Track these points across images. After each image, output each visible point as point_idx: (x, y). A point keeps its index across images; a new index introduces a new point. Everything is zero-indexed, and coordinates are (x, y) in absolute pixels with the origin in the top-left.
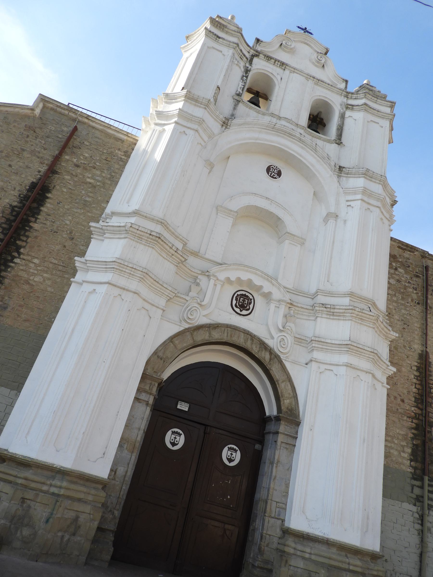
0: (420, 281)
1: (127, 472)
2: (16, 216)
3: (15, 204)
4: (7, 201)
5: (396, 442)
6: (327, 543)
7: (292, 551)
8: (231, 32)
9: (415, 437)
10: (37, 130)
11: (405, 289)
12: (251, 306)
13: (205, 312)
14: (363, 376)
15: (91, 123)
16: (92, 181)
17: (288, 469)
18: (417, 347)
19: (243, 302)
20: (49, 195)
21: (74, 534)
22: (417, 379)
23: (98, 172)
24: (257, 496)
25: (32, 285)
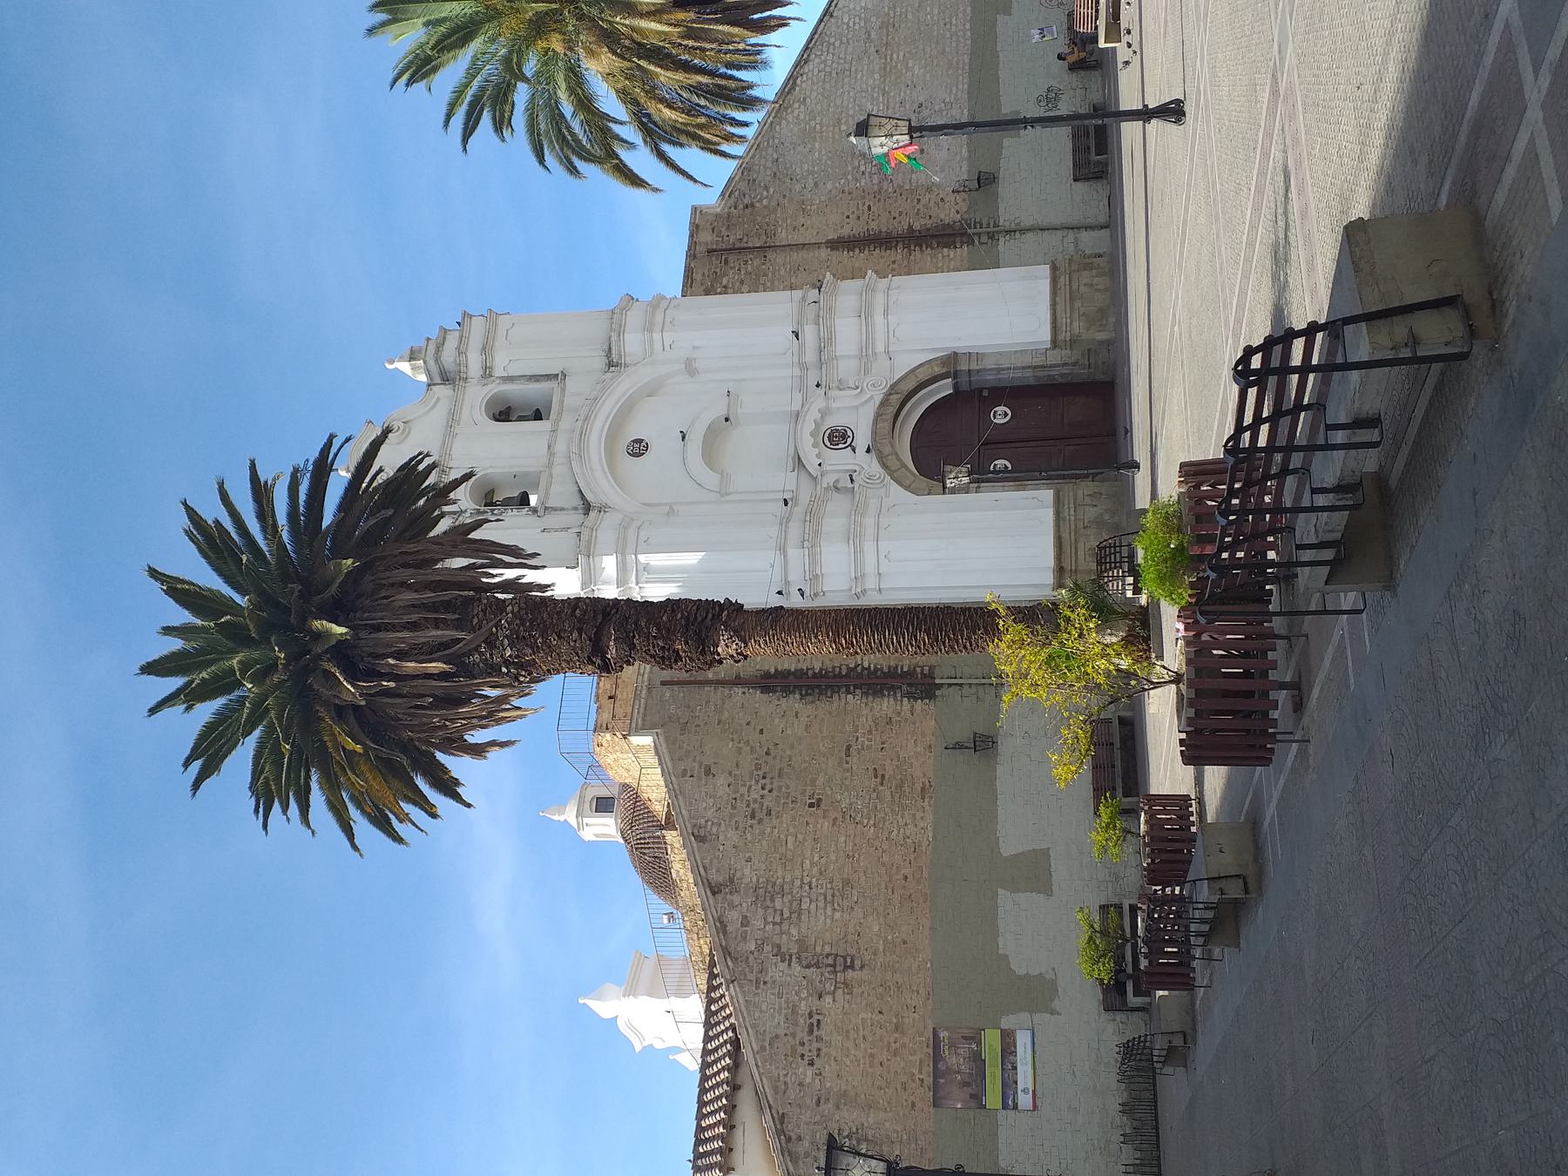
0: (731, 258)
2: (812, 688)
3: (798, 696)
14: (892, 300)
18: (824, 253)
19: (838, 438)
20: (772, 671)
24: (1032, 382)
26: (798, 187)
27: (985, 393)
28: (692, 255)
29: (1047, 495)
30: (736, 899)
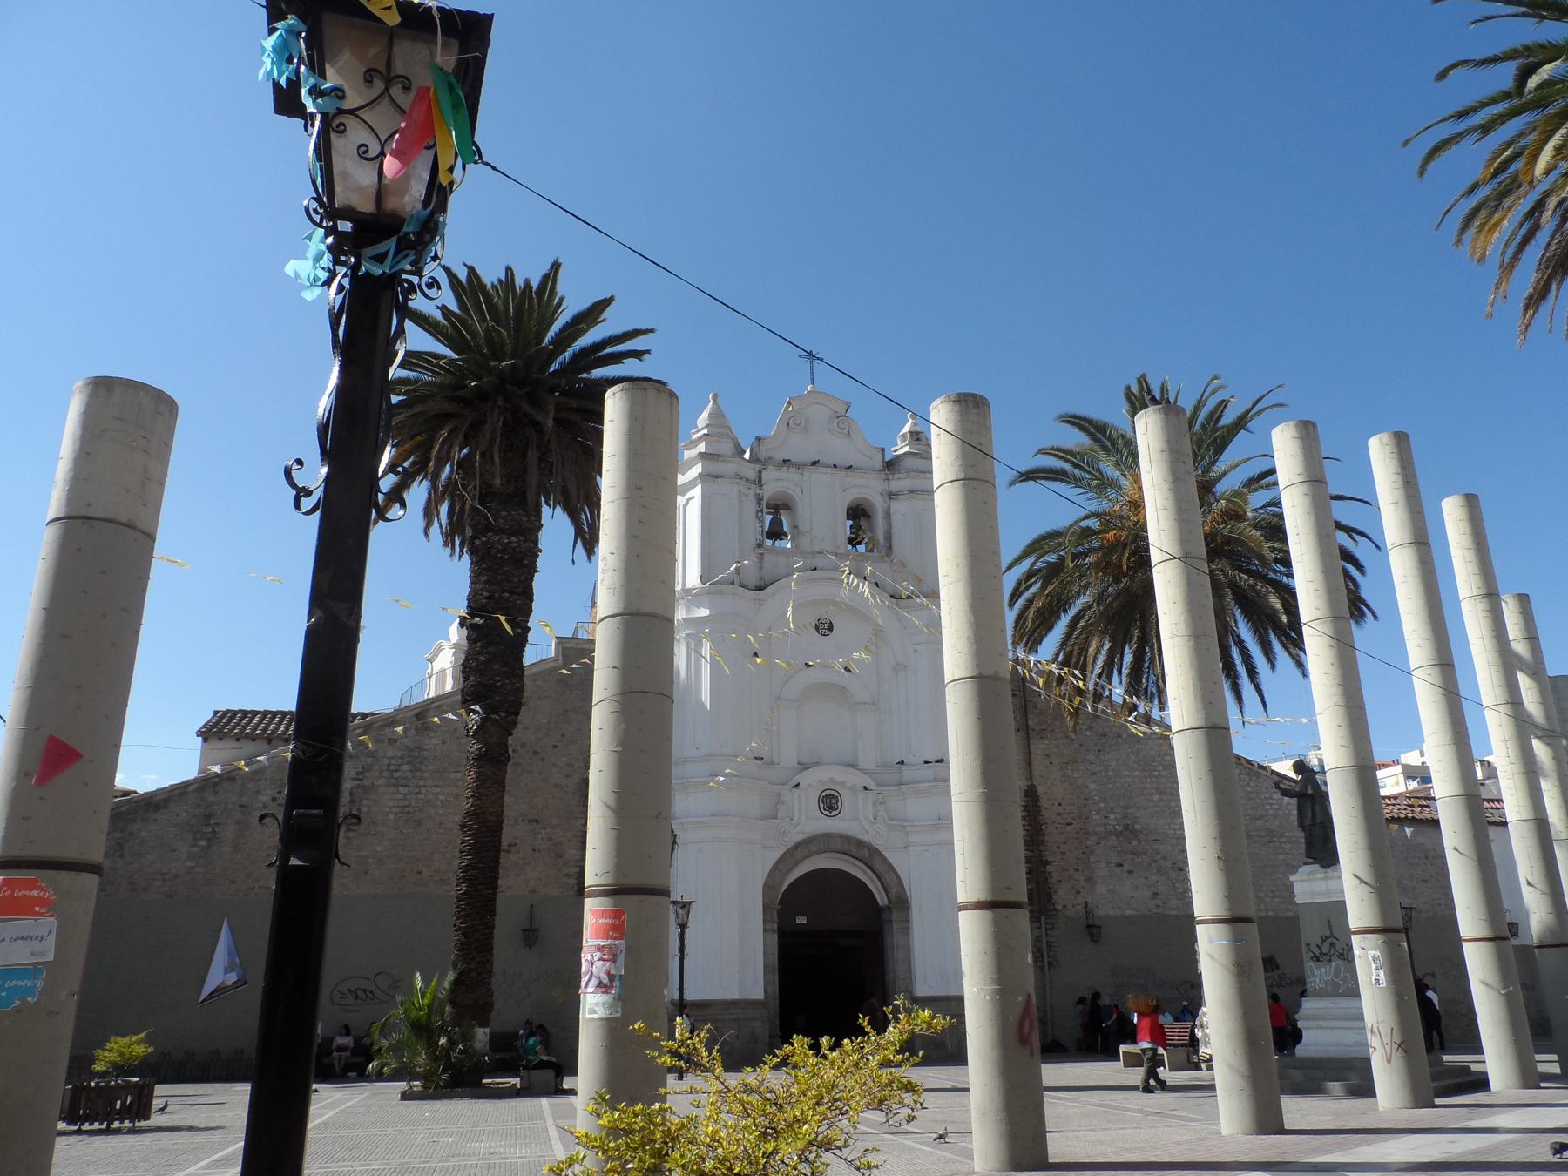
18: (1020, 783)
19: (830, 803)
26: (1091, 757)
29: (758, 993)
30: (412, 733)
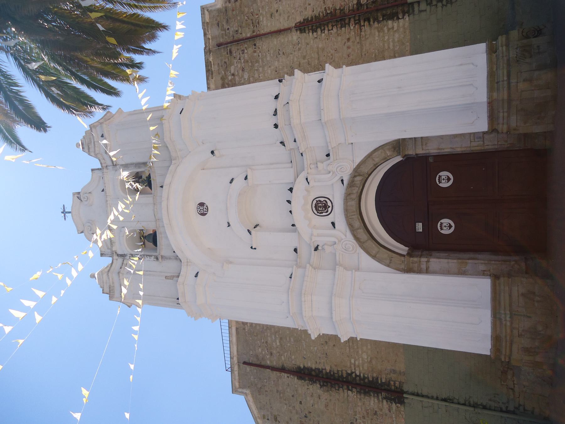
0: (234, 48)
1: (482, 263)
2: (327, 382)
3: (319, 386)
4: (318, 391)
5: (386, 38)
6: (491, 104)
7: (505, 127)
8: (111, 281)
9: (376, 19)
10: (259, 386)
11: (248, 62)
12: (322, 199)
13: (343, 237)
15: (235, 353)
16: (278, 341)
17: (442, 139)
18: (295, 36)
19: (322, 207)
20: (302, 366)
21: (534, 293)
22: (324, 29)
23: (269, 339)
25: (371, 358)
27: (431, 160)
28: (208, 51)
